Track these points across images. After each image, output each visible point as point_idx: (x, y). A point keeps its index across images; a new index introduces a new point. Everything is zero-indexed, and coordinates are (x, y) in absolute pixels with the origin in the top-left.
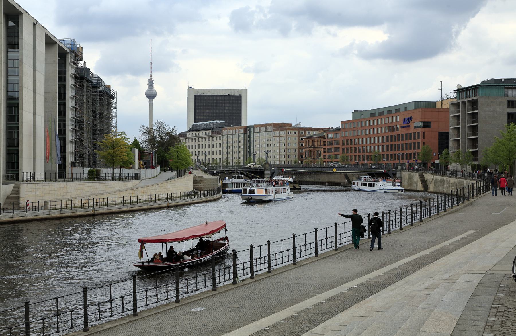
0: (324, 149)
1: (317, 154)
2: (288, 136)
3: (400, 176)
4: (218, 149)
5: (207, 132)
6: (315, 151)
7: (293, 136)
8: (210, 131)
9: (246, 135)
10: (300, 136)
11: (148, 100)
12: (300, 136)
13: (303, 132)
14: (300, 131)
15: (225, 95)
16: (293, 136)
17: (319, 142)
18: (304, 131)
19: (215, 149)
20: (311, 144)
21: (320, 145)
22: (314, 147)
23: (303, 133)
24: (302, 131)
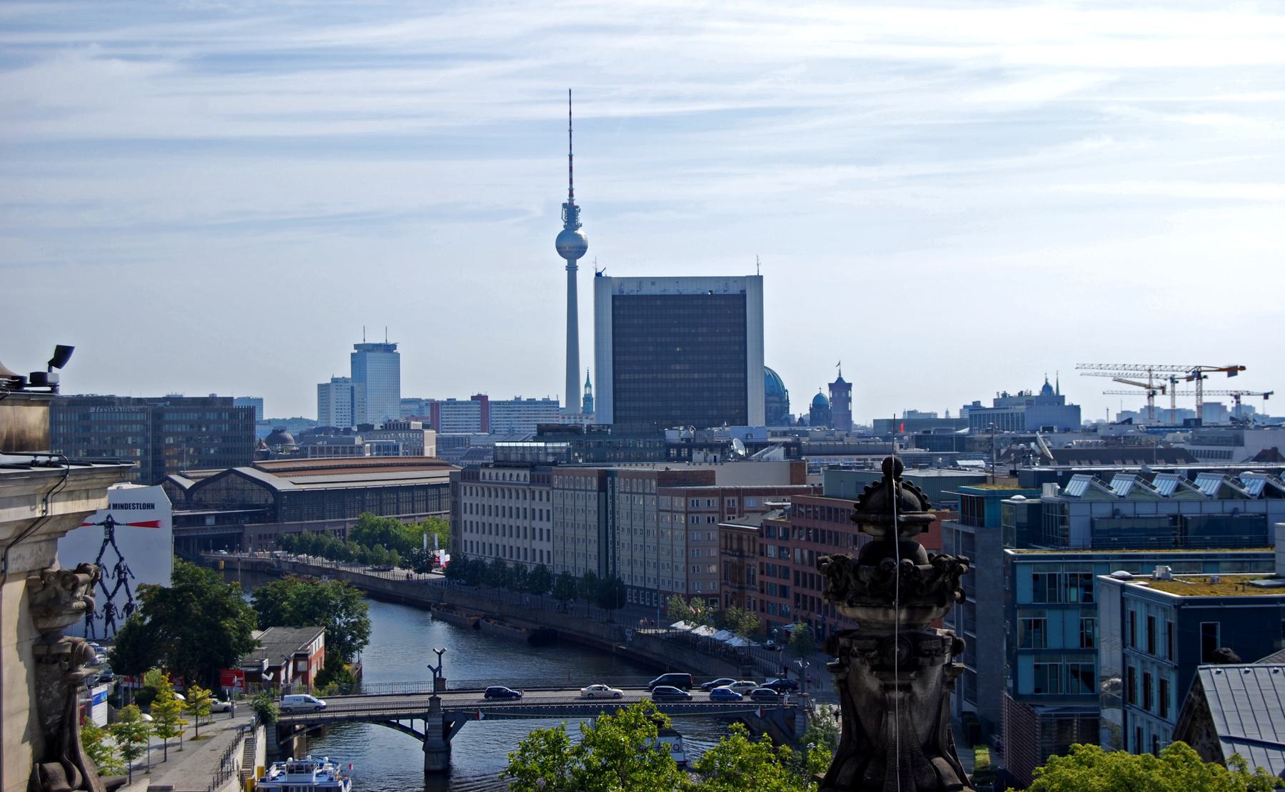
0: (761, 564)
1: (748, 575)
2: (691, 512)
3: (802, 724)
4: (546, 525)
5: (522, 473)
6: (743, 568)
7: (705, 512)
8: (528, 473)
9: (602, 494)
10: (726, 511)
11: (565, 262)
12: (726, 511)
13: (733, 501)
14: (726, 499)
15: (699, 292)
16: (705, 512)
17: (751, 543)
18: (736, 499)
19: (537, 524)
20: (735, 546)
21: (754, 552)
22: (741, 555)
23: (733, 505)
24: (731, 499)
